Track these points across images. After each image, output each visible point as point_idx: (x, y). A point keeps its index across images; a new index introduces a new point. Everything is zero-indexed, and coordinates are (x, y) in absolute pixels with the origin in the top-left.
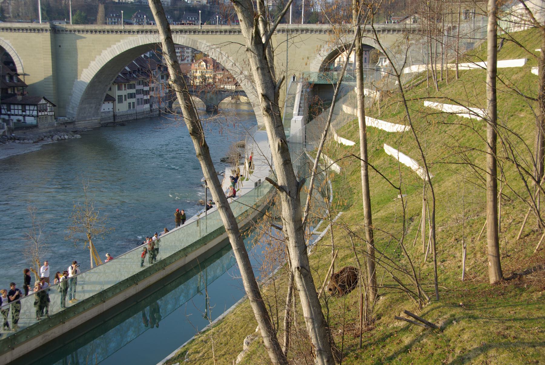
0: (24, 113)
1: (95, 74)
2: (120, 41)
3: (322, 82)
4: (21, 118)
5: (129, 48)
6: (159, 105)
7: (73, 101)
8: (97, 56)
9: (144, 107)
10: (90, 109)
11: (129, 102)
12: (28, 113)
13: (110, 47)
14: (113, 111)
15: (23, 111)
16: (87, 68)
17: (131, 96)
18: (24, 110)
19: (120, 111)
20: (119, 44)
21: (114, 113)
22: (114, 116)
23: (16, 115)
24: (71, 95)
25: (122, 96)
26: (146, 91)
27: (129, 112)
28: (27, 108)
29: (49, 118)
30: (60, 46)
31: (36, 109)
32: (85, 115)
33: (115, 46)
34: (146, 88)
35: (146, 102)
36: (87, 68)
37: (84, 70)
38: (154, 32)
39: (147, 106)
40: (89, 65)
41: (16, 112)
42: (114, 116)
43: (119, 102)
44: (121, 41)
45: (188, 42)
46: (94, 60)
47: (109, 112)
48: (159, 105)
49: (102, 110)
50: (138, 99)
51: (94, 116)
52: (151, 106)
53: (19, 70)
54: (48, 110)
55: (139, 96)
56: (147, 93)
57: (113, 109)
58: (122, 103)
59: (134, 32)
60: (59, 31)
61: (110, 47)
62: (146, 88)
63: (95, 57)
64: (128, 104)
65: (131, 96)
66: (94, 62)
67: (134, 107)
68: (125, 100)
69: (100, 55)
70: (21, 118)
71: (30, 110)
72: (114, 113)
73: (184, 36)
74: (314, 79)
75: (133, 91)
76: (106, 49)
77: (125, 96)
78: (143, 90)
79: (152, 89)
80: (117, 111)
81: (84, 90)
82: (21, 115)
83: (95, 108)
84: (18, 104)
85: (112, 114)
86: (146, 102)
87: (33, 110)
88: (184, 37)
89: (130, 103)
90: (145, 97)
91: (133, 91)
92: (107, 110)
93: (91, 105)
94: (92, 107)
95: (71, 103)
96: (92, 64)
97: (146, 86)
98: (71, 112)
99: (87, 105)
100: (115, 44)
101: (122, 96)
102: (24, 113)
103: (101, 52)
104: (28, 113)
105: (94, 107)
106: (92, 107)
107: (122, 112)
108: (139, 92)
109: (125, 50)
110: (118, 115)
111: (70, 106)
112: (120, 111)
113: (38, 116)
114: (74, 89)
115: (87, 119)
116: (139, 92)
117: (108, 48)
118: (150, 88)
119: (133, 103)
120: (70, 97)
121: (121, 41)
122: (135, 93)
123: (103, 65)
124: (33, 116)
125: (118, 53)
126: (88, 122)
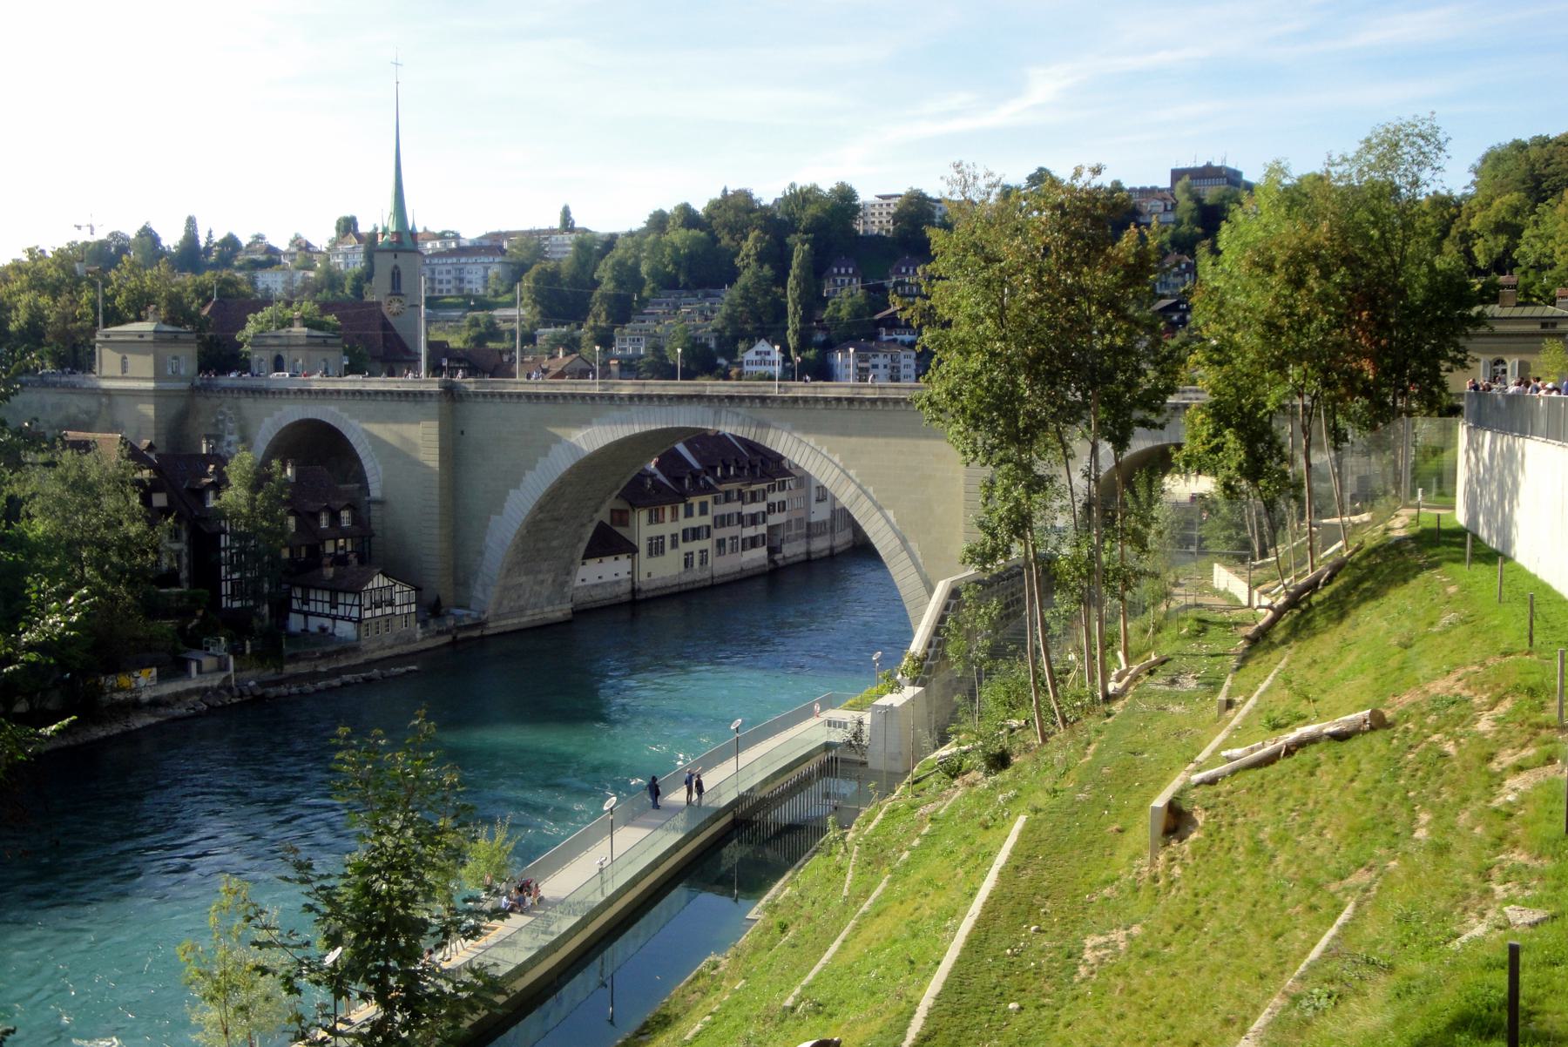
0: (334, 612)
4: (327, 623)
6: (808, 543)
8: (540, 459)
12: (341, 611)
14: (632, 579)
15: (331, 607)
17: (694, 534)
18: (334, 605)
21: (633, 583)
23: (319, 615)
24: (481, 553)
27: (688, 577)
29: (397, 622)
30: (462, 433)
32: (522, 602)
35: (754, 542)
37: (511, 491)
42: (634, 591)
43: (650, 554)
46: (532, 468)
47: (618, 582)
48: (808, 543)
49: (578, 583)
51: (550, 603)
53: (375, 491)
54: (397, 603)
57: (632, 573)
58: (663, 552)
60: (460, 396)
63: (536, 461)
64: (682, 558)
65: (694, 534)
68: (674, 545)
69: (546, 455)
71: (345, 604)
72: (633, 583)
73: (738, 410)
82: (327, 616)
84: (323, 589)
85: (628, 586)
86: (754, 542)
87: (352, 605)
88: (738, 415)
90: (749, 532)
93: (540, 577)
94: (542, 582)
98: (481, 596)
99: (524, 579)
102: (334, 612)
104: (341, 611)
106: (542, 582)
107: (663, 578)
108: (722, 521)
109: (601, 445)
113: (360, 621)
114: (487, 539)
116: (722, 521)
118: (769, 505)
122: (708, 527)
124: (350, 620)
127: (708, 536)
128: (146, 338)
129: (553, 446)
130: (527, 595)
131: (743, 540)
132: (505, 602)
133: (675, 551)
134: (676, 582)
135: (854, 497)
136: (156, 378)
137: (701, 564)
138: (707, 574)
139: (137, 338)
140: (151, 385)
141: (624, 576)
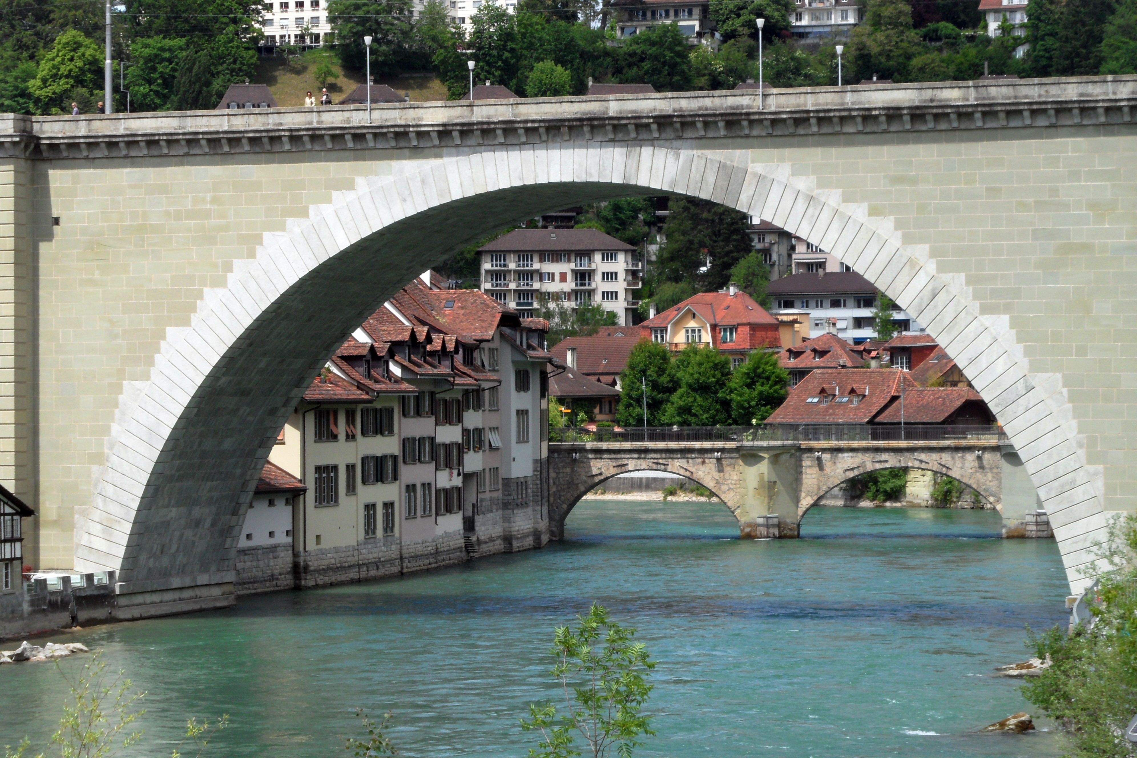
1: (223, 350)
2: (349, 185)
5: (399, 216)
6: (506, 520)
7: (110, 490)
9: (439, 531)
10: (189, 533)
11: (370, 501)
13: (304, 213)
16: (186, 322)
19: (325, 544)
20: (350, 196)
21: (296, 555)
24: (99, 458)
25: (335, 468)
26: (447, 447)
27: (369, 554)
33: (327, 210)
36: (186, 322)
38: (527, 130)
40: (194, 309)
44: (360, 181)
45: (696, 175)
46: (220, 282)
47: (273, 549)
48: (506, 520)
50: (411, 488)
51: (204, 568)
52: (469, 525)
57: (292, 533)
58: (336, 501)
59: (421, 135)
61: (304, 213)
63: (229, 268)
64: (362, 512)
66: (221, 292)
67: (389, 527)
68: (351, 489)
69: (252, 255)
72: (296, 555)
76: (282, 228)
77: (350, 468)
78: (432, 439)
80: (311, 545)
81: (166, 433)
83: (213, 524)
89: (370, 508)
92: (261, 540)
93: (197, 512)
94: (198, 523)
95: (99, 501)
97: (448, 420)
99: (173, 513)
100: (328, 200)
101: (335, 468)
103: (258, 240)
105: (208, 524)
106: (198, 523)
107: (337, 550)
109: (377, 227)
110: (313, 565)
111: (97, 515)
112: (325, 544)
114: (115, 428)
115: (176, 582)
117: (290, 222)
119: (389, 506)
120: (95, 468)
121: (360, 181)
122: (395, 458)
123: (265, 305)
126: (176, 595)
127: (395, 478)
129: (267, 236)
130: (174, 547)
131: (438, 491)
132: (143, 557)
133: (352, 499)
134: (353, 560)
135: (927, 294)
137: (385, 530)
138: (393, 552)
141: (282, 539)
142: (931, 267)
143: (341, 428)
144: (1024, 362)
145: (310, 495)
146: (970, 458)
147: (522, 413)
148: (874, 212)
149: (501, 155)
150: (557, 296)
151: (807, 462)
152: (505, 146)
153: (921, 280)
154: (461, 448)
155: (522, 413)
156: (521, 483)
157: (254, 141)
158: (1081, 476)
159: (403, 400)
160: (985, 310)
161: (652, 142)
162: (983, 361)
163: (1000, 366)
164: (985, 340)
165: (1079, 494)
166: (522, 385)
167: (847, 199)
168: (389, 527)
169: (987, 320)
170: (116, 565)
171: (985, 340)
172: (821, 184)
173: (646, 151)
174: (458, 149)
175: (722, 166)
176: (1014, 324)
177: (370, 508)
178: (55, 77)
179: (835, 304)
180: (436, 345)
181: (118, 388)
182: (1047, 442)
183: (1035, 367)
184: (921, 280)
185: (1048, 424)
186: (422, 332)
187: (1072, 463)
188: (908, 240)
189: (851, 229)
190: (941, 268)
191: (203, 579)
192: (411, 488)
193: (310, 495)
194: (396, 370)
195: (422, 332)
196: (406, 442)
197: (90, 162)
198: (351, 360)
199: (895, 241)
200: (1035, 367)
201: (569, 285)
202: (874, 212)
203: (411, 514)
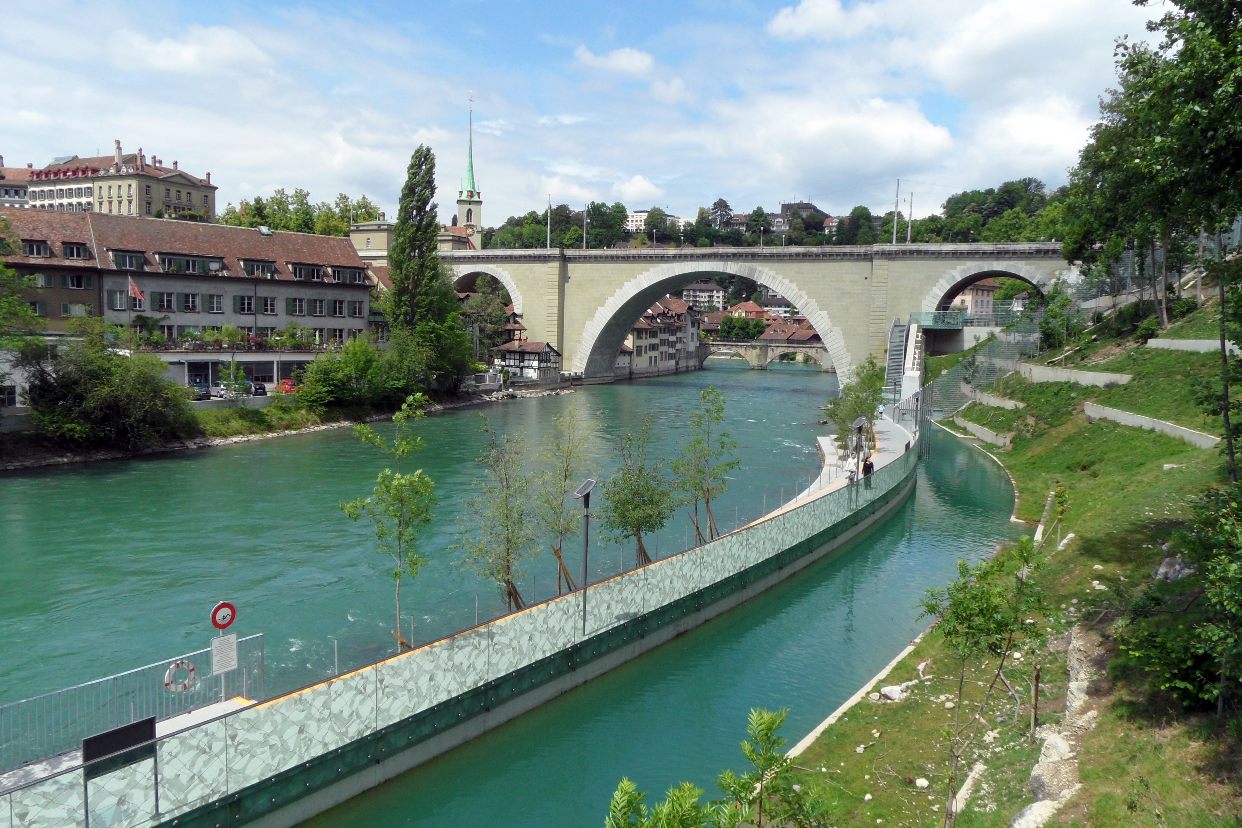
0: (522, 364)
2: (648, 270)
3: (940, 326)
4: (518, 370)
13: (636, 277)
17: (653, 347)
18: (522, 360)
20: (648, 273)
22: (631, 373)
24: (579, 342)
27: (650, 370)
28: (526, 357)
31: (537, 358)
33: (642, 277)
34: (672, 338)
35: (672, 356)
39: (672, 363)
41: (512, 364)
42: (631, 373)
46: (612, 295)
49: (617, 366)
50: (662, 353)
51: (606, 372)
52: (677, 363)
55: (663, 349)
56: (672, 344)
57: (630, 363)
61: (636, 277)
62: (672, 338)
63: (615, 292)
65: (653, 347)
66: (613, 298)
67: (655, 363)
68: (646, 352)
70: (518, 370)
74: (928, 323)
75: (655, 341)
79: (679, 340)
82: (518, 367)
85: (628, 370)
89: (651, 357)
90: (671, 351)
91: (655, 341)
92: (621, 365)
93: (605, 357)
94: (604, 360)
96: (610, 300)
97: (672, 335)
98: (579, 365)
108: (663, 342)
116: (663, 342)
119: (655, 357)
125: (646, 286)
128: (382, 227)
136: (388, 250)
138: (656, 369)
139: (376, 228)
140: (385, 253)
141: (627, 365)
142: (806, 297)
143: (644, 336)
144: (830, 324)
145: (635, 353)
146: (814, 350)
147: (692, 334)
148: (791, 281)
149: (689, 263)
150: (703, 302)
151: (769, 349)
152: (691, 261)
153: (803, 301)
154: (676, 342)
155: (692, 334)
156: (692, 352)
157: (623, 258)
158: (844, 356)
159: (661, 329)
160: (820, 309)
161: (731, 261)
162: (819, 324)
163: (823, 325)
164: (820, 318)
165: (844, 361)
166: (693, 326)
167: (783, 278)
168: (655, 363)
169: (821, 312)
170: (583, 370)
171: (820, 318)
172: (777, 273)
173: (729, 263)
174: (678, 261)
175: (750, 268)
176: (828, 313)
177: (651, 357)
178: (571, 239)
179: (779, 307)
180: (670, 314)
181: (585, 323)
182: (835, 346)
183: (834, 325)
184: (803, 301)
185: (836, 341)
186: (666, 311)
187: (842, 352)
188: (800, 289)
189: (784, 286)
190: (809, 297)
191: (606, 375)
192: (662, 353)
193: (635, 353)
194: (659, 321)
195: (666, 311)
196: (661, 340)
197: (579, 262)
198: (647, 317)
199: (796, 290)
200: (834, 325)
201: (707, 299)
202: (791, 281)
203: (662, 359)
